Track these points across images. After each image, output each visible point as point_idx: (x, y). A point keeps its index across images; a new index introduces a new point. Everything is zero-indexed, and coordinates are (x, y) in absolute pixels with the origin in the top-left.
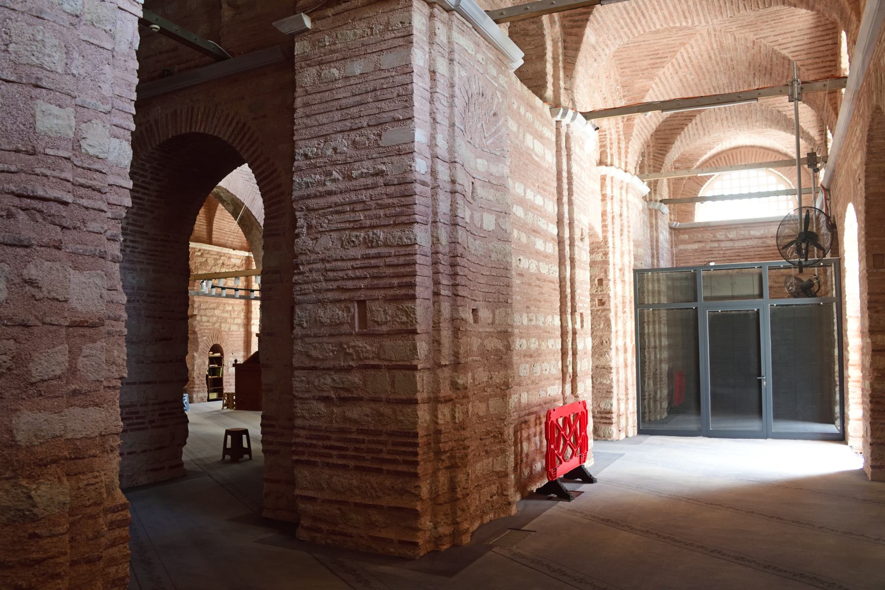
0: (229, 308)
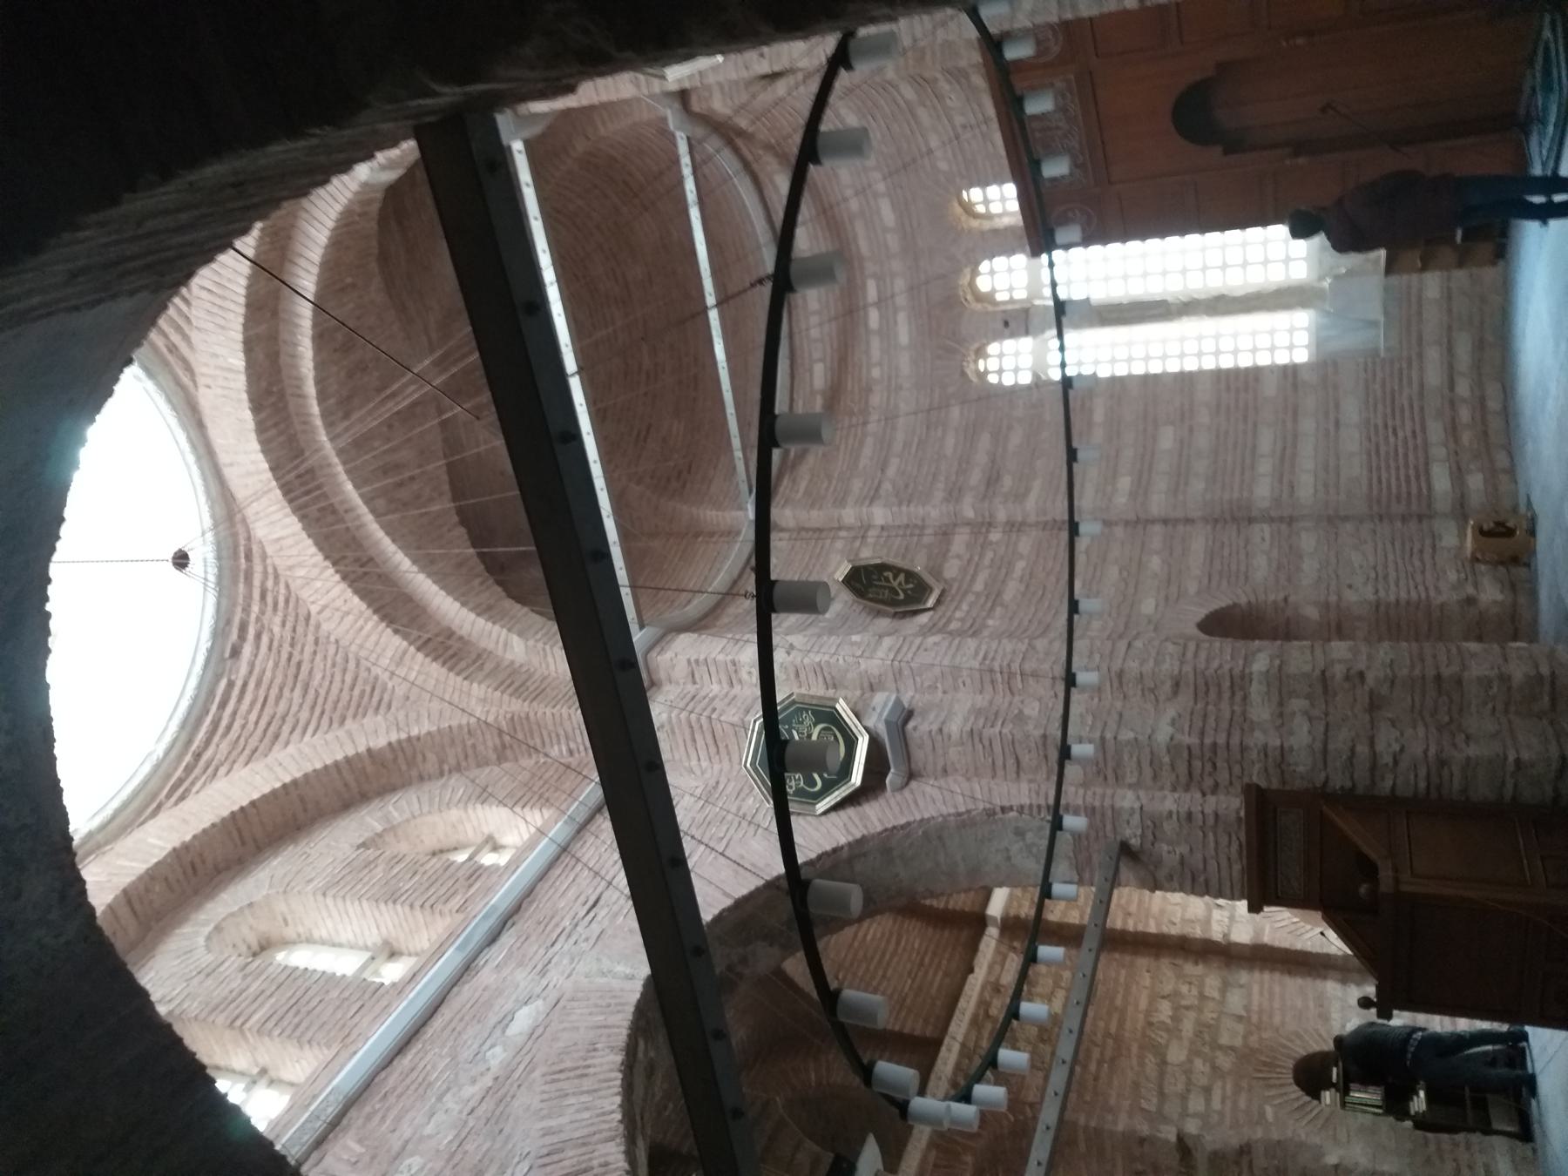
0: (1165, 1010)
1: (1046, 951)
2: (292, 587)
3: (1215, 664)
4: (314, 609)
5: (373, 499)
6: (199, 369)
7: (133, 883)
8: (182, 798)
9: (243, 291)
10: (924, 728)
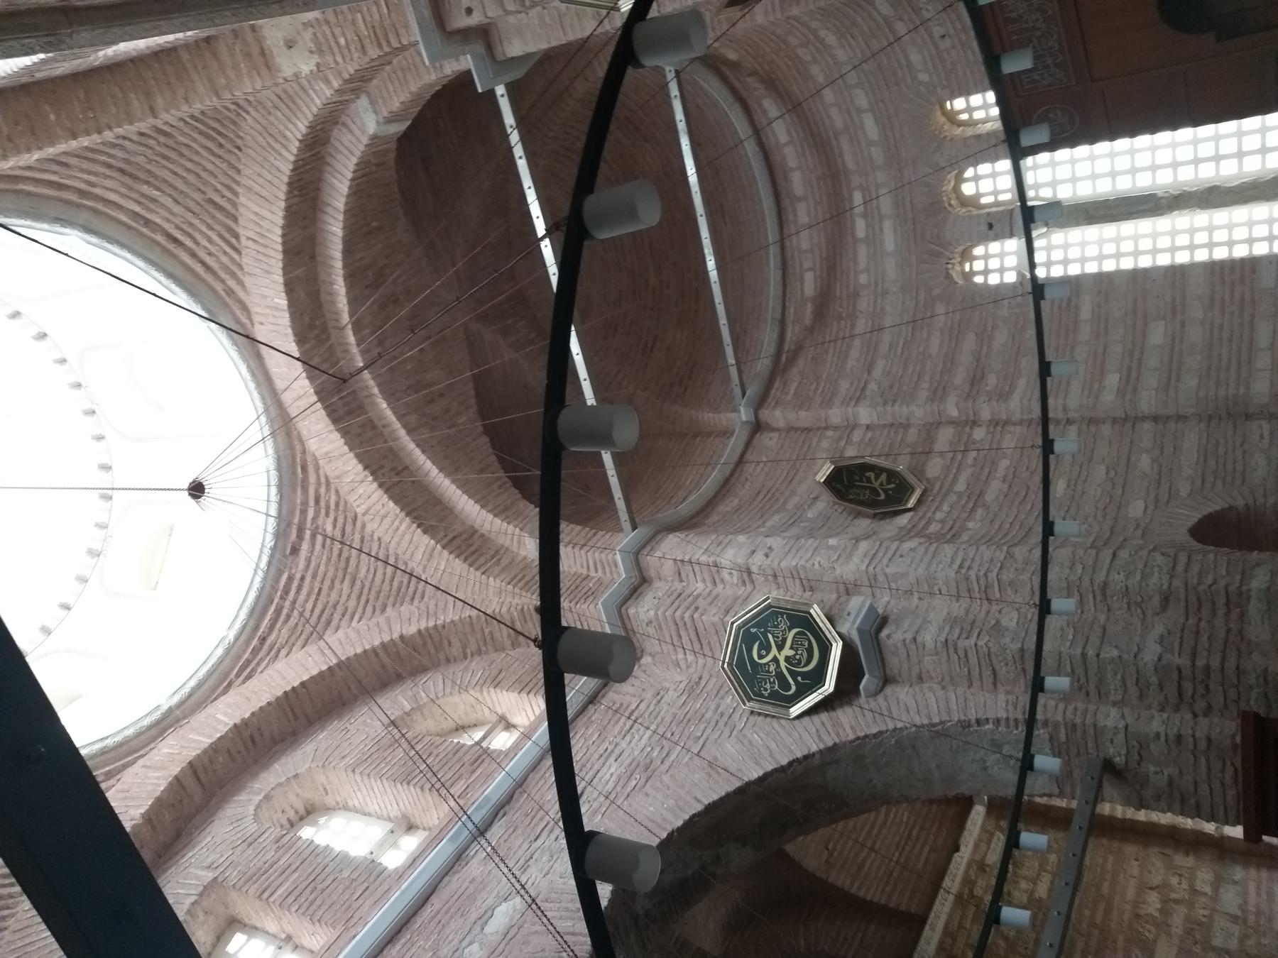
0: (1153, 903)
1: (1030, 838)
2: (342, 494)
3: (1210, 578)
4: (360, 510)
5: (405, 415)
6: (254, 309)
7: (198, 756)
8: (249, 677)
9: (279, 240)
10: (898, 636)
